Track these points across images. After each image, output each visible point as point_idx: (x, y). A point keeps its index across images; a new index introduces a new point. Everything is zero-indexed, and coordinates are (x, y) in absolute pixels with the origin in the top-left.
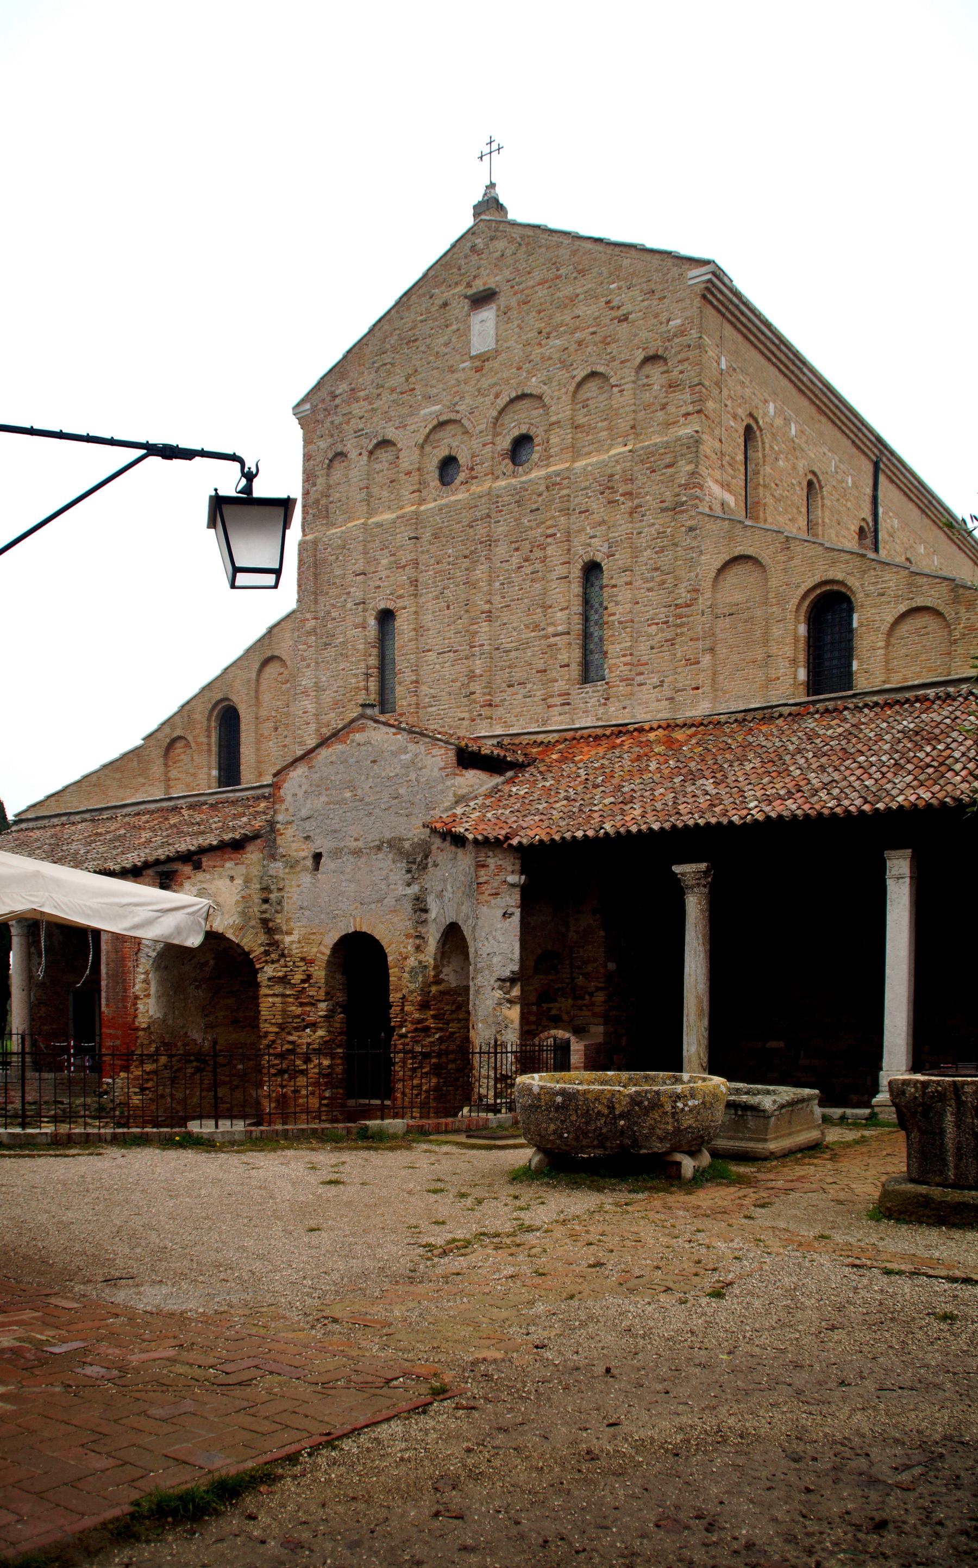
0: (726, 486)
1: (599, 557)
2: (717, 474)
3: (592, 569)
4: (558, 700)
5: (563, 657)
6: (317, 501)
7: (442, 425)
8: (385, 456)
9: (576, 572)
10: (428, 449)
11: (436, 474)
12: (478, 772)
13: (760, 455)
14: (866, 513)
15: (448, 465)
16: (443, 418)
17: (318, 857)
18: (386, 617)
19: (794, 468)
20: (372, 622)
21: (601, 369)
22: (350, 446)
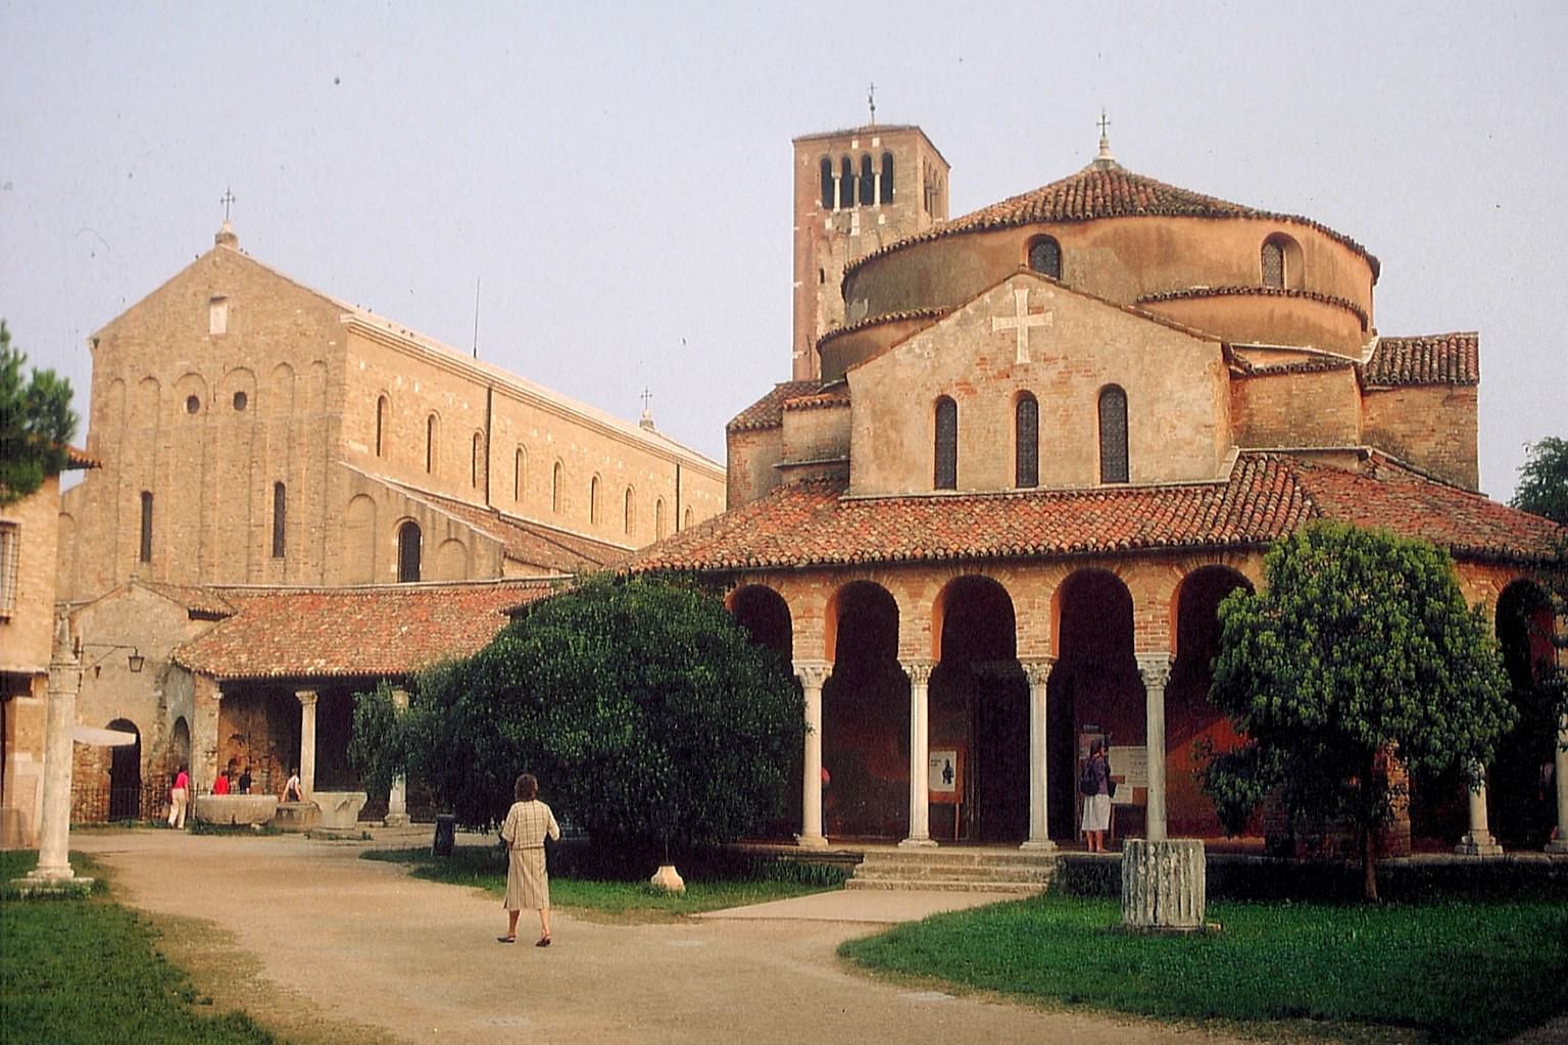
0: (363, 441)
1: (284, 481)
2: (357, 436)
3: (279, 487)
4: (256, 568)
5: (259, 540)
6: (101, 410)
7: (189, 374)
8: (152, 387)
9: (270, 489)
10: (179, 388)
11: (185, 405)
12: (201, 622)
13: (390, 412)
14: (481, 423)
15: (193, 402)
16: (191, 371)
17: (98, 669)
18: (147, 497)
19: (417, 412)
20: (138, 500)
21: (287, 362)
22: (126, 375)
